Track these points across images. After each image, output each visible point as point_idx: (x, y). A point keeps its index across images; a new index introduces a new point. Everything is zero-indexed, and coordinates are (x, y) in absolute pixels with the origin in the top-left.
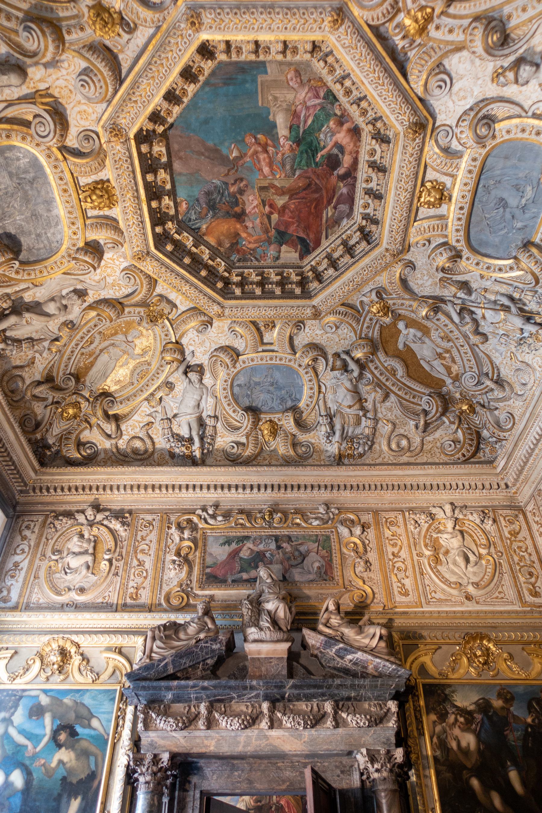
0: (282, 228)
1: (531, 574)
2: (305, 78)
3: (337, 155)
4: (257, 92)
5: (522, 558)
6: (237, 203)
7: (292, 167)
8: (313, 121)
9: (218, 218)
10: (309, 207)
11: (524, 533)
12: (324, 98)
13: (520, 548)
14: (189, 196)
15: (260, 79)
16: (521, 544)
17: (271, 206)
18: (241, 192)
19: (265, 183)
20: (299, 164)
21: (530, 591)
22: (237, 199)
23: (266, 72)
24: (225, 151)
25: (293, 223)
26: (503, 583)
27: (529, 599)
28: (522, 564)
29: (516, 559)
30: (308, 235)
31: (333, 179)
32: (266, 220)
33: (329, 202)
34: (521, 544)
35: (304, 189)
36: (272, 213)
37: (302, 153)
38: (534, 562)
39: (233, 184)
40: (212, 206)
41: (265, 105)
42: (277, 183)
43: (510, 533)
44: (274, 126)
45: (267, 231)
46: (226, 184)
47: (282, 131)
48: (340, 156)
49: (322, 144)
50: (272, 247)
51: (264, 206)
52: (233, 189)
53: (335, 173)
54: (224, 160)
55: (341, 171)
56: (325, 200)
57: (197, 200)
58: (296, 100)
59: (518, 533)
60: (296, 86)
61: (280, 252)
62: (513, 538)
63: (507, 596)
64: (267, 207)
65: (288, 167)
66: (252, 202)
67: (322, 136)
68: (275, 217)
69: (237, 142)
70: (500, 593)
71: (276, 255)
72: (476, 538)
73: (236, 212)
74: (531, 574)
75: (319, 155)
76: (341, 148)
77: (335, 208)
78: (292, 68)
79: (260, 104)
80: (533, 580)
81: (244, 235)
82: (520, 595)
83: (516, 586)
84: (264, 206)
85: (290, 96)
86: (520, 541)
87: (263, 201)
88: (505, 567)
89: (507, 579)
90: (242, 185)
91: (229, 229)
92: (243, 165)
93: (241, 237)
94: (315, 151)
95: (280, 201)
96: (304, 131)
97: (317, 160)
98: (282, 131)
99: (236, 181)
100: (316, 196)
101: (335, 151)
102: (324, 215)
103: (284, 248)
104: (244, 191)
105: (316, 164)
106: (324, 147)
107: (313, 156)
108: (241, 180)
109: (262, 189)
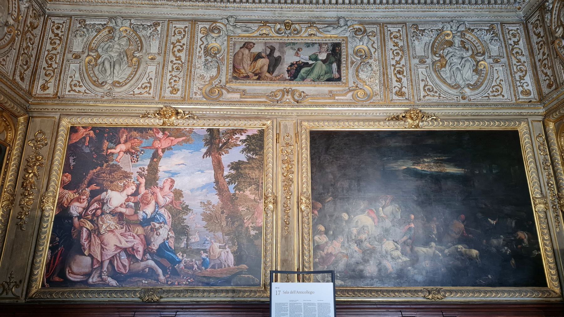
1: (27, 62)
5: (28, 47)
11: (37, 32)
13: (30, 39)
16: (32, 37)
21: (21, 74)
26: (9, 55)
27: (18, 79)
28: (26, 51)
29: (25, 45)
34: (32, 37)
38: (32, 56)
43: (31, 23)
59: (35, 28)
62: (30, 29)
63: (6, 66)
70: (4, 60)
72: (10, 5)
74: (27, 62)
80: (25, 67)
82: (14, 71)
83: (16, 64)
86: (33, 35)
88: (17, 45)
89: (14, 53)
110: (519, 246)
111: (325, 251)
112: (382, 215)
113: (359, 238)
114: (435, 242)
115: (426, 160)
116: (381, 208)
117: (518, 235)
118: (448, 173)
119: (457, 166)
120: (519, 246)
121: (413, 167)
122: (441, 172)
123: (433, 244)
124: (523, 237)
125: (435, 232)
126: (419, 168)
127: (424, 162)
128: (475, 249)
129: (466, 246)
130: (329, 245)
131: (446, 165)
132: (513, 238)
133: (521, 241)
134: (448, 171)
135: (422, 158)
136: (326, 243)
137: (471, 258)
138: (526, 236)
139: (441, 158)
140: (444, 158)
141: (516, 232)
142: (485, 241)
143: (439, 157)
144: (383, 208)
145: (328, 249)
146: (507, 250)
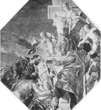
0: (59, 86)
2: (70, 7)
3: (89, 44)
4: (47, 12)
6: (33, 71)
7: (65, 50)
8: (76, 26)
9: (22, 79)
10: (75, 73)
12: (80, 16)
14: (7, 66)
15: (49, 6)
17: (53, 72)
18: (37, 63)
19: (50, 59)
20: (69, 49)
22: (34, 68)
23: (52, 4)
24: (29, 41)
25: (66, 83)
30: (75, 92)
31: (88, 57)
32: (50, 81)
33: (86, 71)
35: (72, 63)
36: (54, 77)
37: (70, 42)
39: (32, 59)
40: (20, 72)
41: (51, 18)
42: (56, 58)
44: (55, 28)
45: (50, 89)
46: (28, 59)
47: (60, 31)
48: (91, 44)
49: (81, 38)
50: (54, 99)
51: (49, 72)
52: (32, 62)
53: (89, 53)
54: (28, 45)
55: (92, 52)
56: (84, 70)
57: (11, 68)
58: (67, 17)
60: (66, 10)
61: (58, 103)
64: (51, 73)
65: (63, 50)
66: (41, 69)
67: (80, 34)
68: (55, 79)
69: (36, 36)
71: (56, 104)
73: (33, 76)
75: (80, 43)
76: (91, 40)
77: (90, 74)
78: (65, 3)
79: (48, 18)
81: (36, 90)
84: (49, 72)
85: (63, 15)
87: (49, 69)
90: (37, 59)
91: (28, 87)
92: (38, 48)
93: (35, 93)
94: (77, 42)
95: (59, 69)
96: (71, 31)
97: (79, 46)
98: (60, 31)
99: (34, 57)
100: (79, 66)
101: (88, 42)
102: (84, 78)
103: (61, 100)
104: (38, 63)
105: (78, 48)
106: (82, 40)
107: (76, 44)
108: (37, 56)
109: (49, 62)
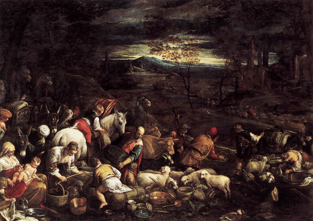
110: (288, 171)
111: (15, 179)
112: (99, 128)
113: (63, 161)
114: (171, 166)
115: (171, 45)
116: (97, 119)
117: (288, 156)
118: (201, 65)
119: (218, 53)
120: (288, 171)
121: (151, 56)
122: (190, 64)
123: (167, 169)
124: (295, 159)
125: (172, 152)
126: (159, 57)
127: (168, 48)
128: (225, 174)
129: (213, 171)
130: (20, 170)
131: (200, 53)
132: (280, 161)
133: (292, 163)
134: (201, 62)
135: (166, 42)
136: (17, 167)
137: (217, 188)
138: (300, 157)
139: (194, 42)
140: (199, 42)
141: (288, 150)
142: (240, 164)
143: (191, 40)
144: (101, 118)
145: (18, 177)
146: (269, 177)
